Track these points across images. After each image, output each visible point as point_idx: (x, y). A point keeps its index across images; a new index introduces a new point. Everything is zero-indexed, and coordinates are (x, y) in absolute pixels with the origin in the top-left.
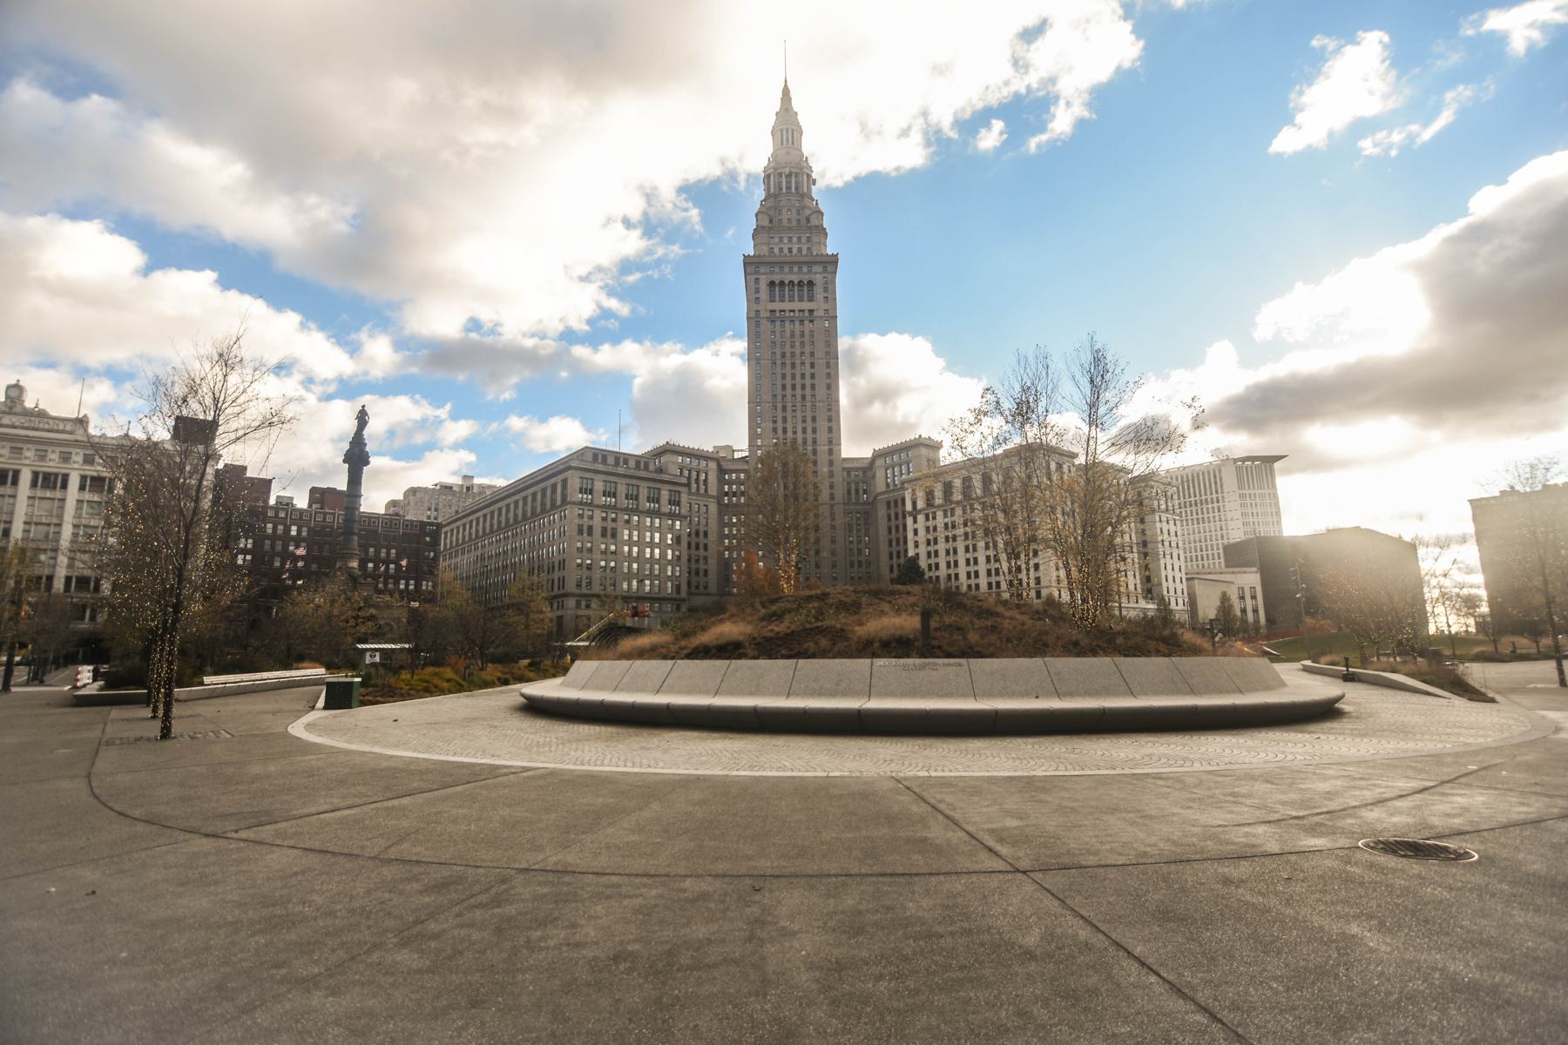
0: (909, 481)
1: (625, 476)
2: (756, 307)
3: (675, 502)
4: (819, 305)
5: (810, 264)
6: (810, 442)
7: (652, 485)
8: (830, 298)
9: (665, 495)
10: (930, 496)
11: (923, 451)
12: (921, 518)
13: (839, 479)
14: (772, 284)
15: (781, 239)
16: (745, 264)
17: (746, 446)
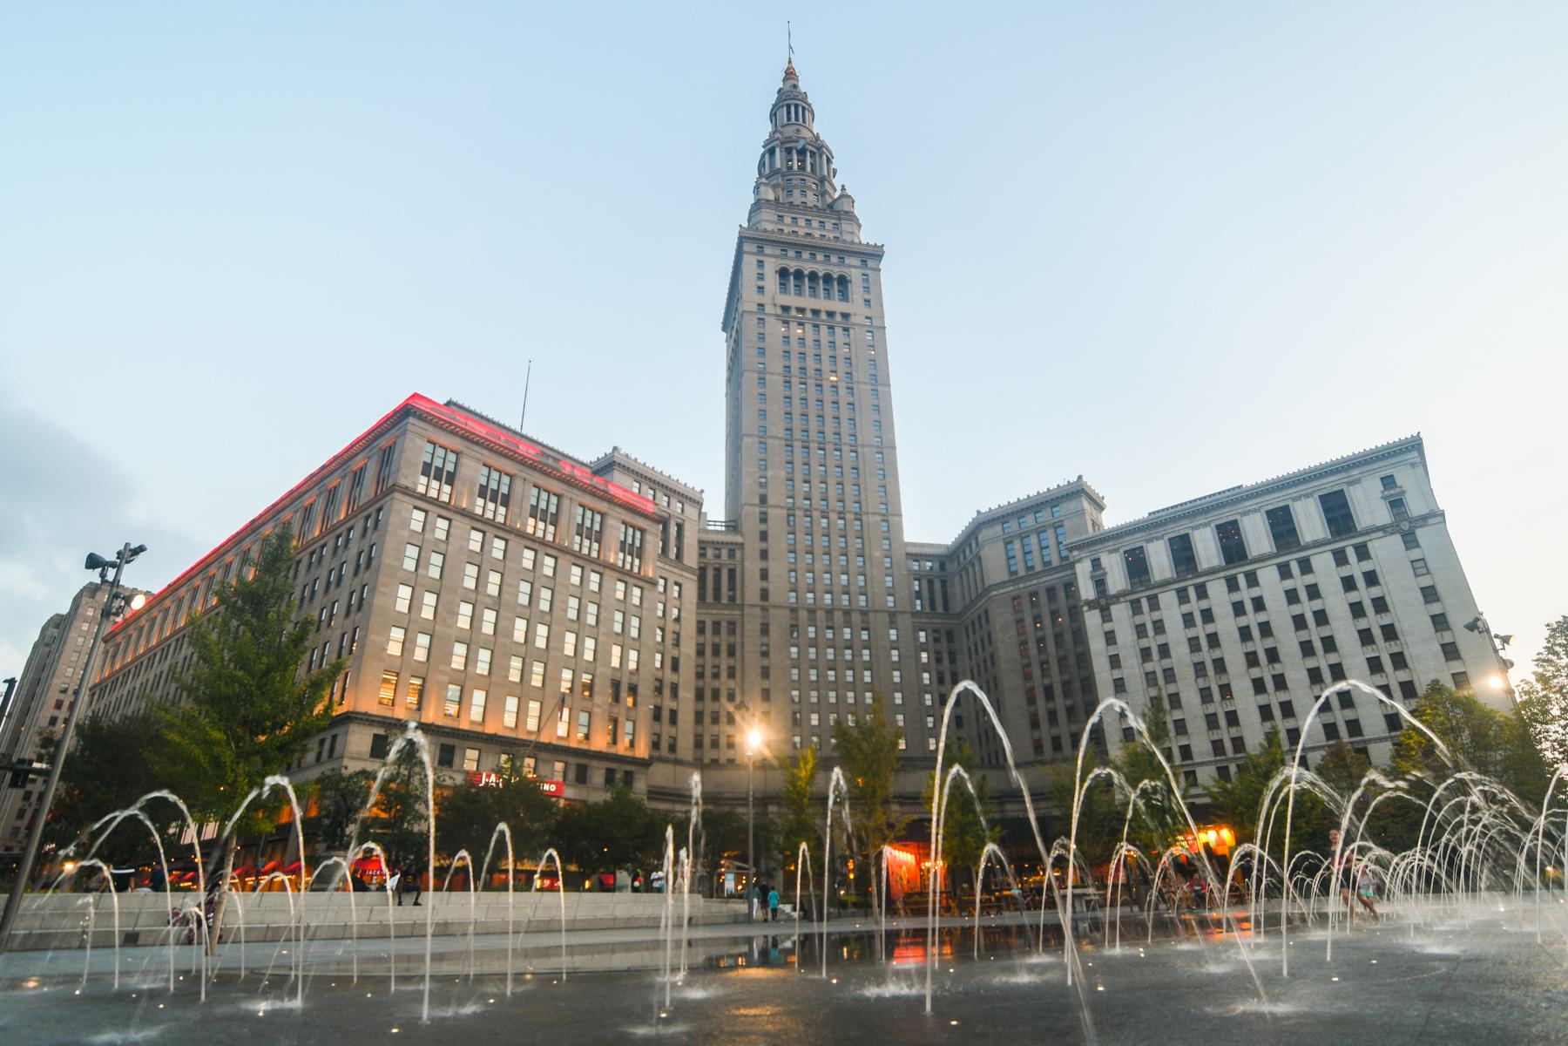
0: (1080, 546)
1: (533, 466)
2: (760, 299)
4: (855, 306)
5: (843, 253)
8: (872, 300)
9: (616, 531)
10: (1137, 565)
11: (1086, 504)
12: (1120, 611)
14: (783, 273)
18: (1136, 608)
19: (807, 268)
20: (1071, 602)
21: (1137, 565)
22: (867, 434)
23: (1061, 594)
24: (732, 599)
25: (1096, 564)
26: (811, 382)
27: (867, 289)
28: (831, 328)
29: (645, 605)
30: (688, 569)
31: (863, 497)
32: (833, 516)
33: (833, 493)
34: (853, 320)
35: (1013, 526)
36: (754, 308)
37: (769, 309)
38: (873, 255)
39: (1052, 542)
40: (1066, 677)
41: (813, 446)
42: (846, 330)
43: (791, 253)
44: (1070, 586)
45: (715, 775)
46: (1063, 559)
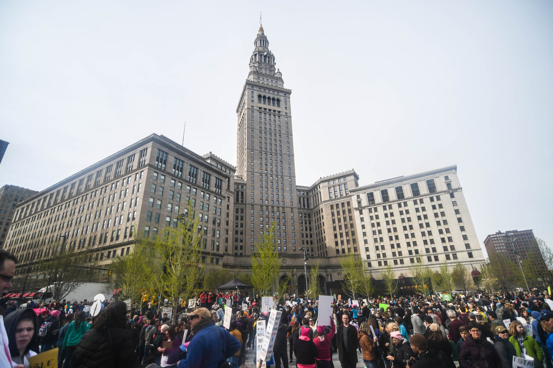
3: (219, 186)
4: (282, 109)
6: (280, 173)
7: (206, 170)
10: (371, 197)
12: (366, 211)
13: (295, 194)
14: (260, 96)
16: (248, 83)
18: (370, 211)
19: (267, 95)
20: (349, 208)
21: (371, 197)
22: (285, 151)
23: (346, 205)
24: (242, 201)
25: (358, 197)
26: (268, 133)
27: (286, 104)
28: (274, 115)
29: (222, 205)
30: (231, 192)
31: (283, 171)
32: (274, 176)
33: (274, 169)
34: (281, 113)
35: (331, 183)
36: (250, 107)
37: (255, 108)
39: (343, 188)
40: (347, 231)
41: (269, 153)
42: (279, 116)
43: (262, 90)
44: (349, 203)
45: (239, 259)
46: (346, 194)
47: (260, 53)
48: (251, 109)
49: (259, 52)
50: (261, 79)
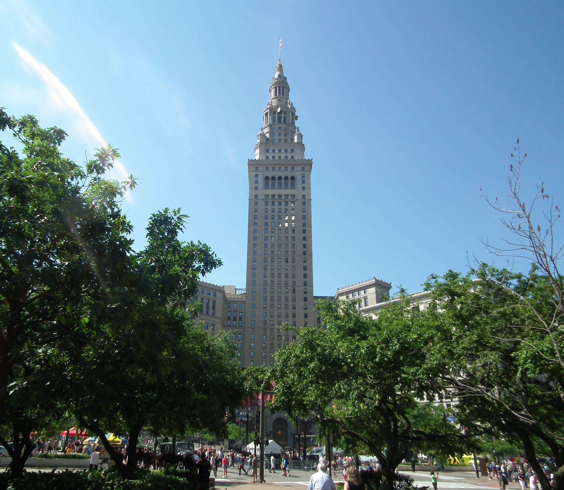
5: (293, 165)
6: (290, 284)
8: (306, 186)
14: (267, 178)
15: (274, 151)
16: (249, 165)
17: (244, 287)
19: (277, 174)
27: (303, 182)
34: (296, 197)
37: (259, 197)
38: (309, 164)
43: (270, 169)
47: (272, 111)
48: (254, 202)
49: (271, 109)
50: (271, 151)
